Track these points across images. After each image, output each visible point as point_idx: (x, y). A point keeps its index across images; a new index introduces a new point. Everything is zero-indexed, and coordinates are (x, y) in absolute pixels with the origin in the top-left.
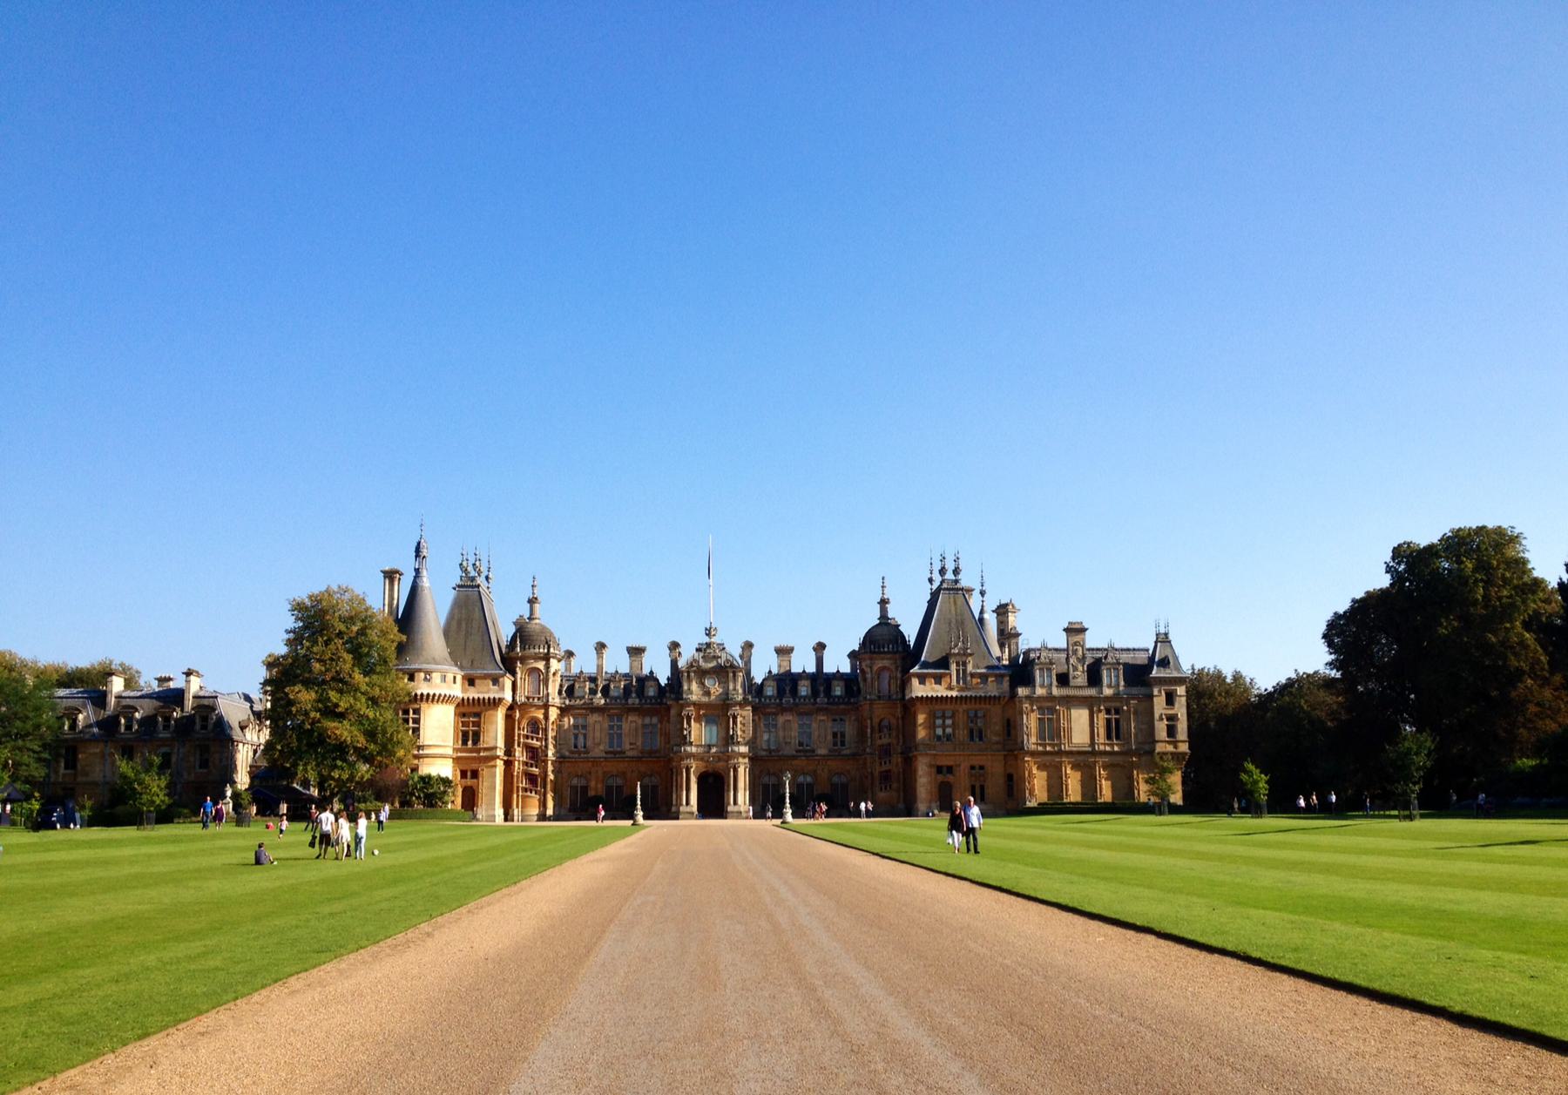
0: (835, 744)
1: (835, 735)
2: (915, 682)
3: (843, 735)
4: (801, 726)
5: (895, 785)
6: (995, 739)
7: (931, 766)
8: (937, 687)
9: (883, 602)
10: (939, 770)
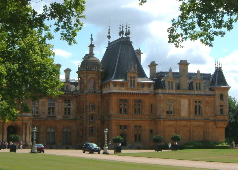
0: (65, 113)
1: (65, 109)
2: (111, 85)
3: (69, 109)
4: (50, 104)
5: (96, 134)
8: (122, 88)
10: (121, 127)
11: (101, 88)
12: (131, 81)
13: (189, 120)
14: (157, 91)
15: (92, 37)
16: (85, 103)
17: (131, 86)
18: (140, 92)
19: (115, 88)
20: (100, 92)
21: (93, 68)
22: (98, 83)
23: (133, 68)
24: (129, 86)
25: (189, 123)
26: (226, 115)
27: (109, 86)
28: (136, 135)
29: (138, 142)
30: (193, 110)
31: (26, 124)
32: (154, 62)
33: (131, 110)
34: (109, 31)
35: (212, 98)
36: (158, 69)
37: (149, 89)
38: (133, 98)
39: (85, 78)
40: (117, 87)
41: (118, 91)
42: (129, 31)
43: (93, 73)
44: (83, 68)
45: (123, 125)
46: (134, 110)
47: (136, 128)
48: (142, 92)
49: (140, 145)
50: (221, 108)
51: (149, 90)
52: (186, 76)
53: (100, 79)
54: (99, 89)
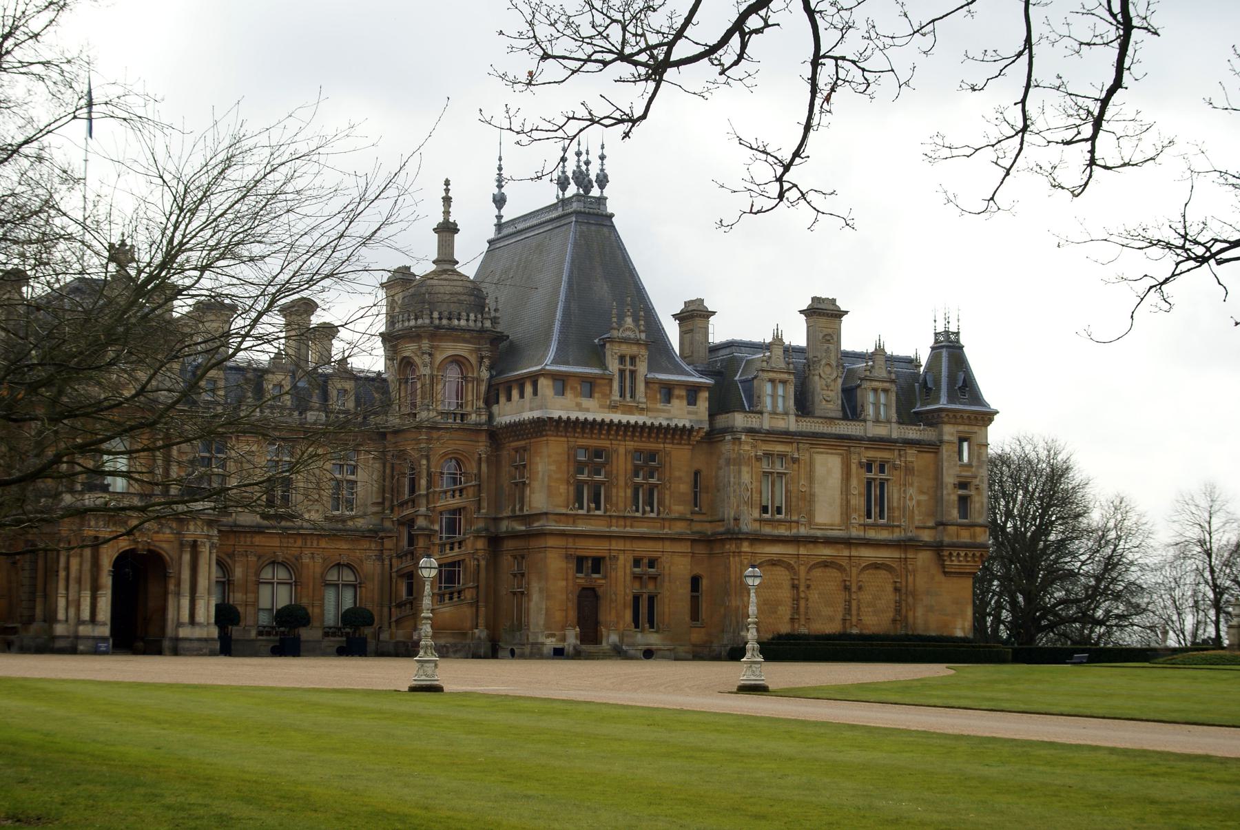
5: (468, 595)
6: (678, 509)
7: (568, 557)
8: (586, 402)
9: (447, 230)
10: (580, 561)
11: (491, 399)
12: (622, 372)
13: (848, 542)
14: (722, 421)
15: (447, 190)
16: (424, 462)
17: (622, 395)
18: (656, 423)
19: (560, 400)
20: (484, 418)
21: (459, 319)
22: (479, 380)
23: (629, 320)
24: (616, 396)
25: (846, 553)
26: (981, 526)
27: (535, 393)
28: (636, 599)
29: (647, 625)
30: (858, 502)
31: (194, 545)
32: (703, 301)
33: (622, 494)
34: (500, 175)
35: (928, 457)
36: (718, 332)
37: (691, 408)
38: (631, 445)
39: (427, 358)
40: (569, 394)
41: (573, 417)
42: (602, 170)
43: (456, 340)
44: (416, 319)
45: (587, 558)
46: (629, 492)
47: (637, 570)
48: (665, 423)
49: (653, 639)
50: (960, 492)
51: (689, 413)
52: (834, 363)
53: (487, 361)
54: (482, 404)
